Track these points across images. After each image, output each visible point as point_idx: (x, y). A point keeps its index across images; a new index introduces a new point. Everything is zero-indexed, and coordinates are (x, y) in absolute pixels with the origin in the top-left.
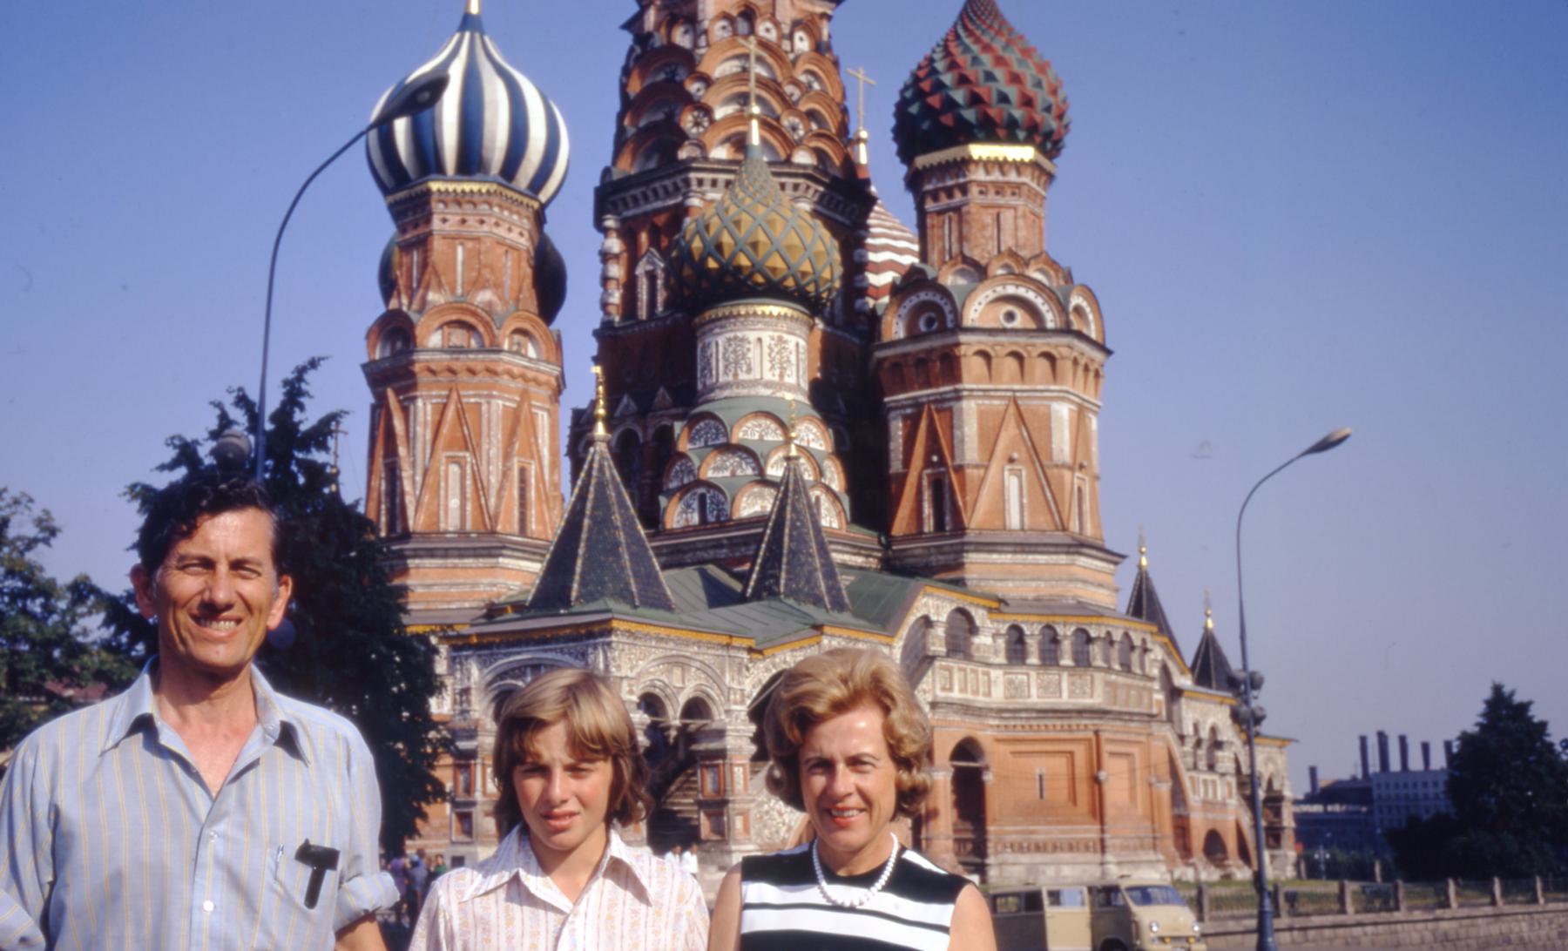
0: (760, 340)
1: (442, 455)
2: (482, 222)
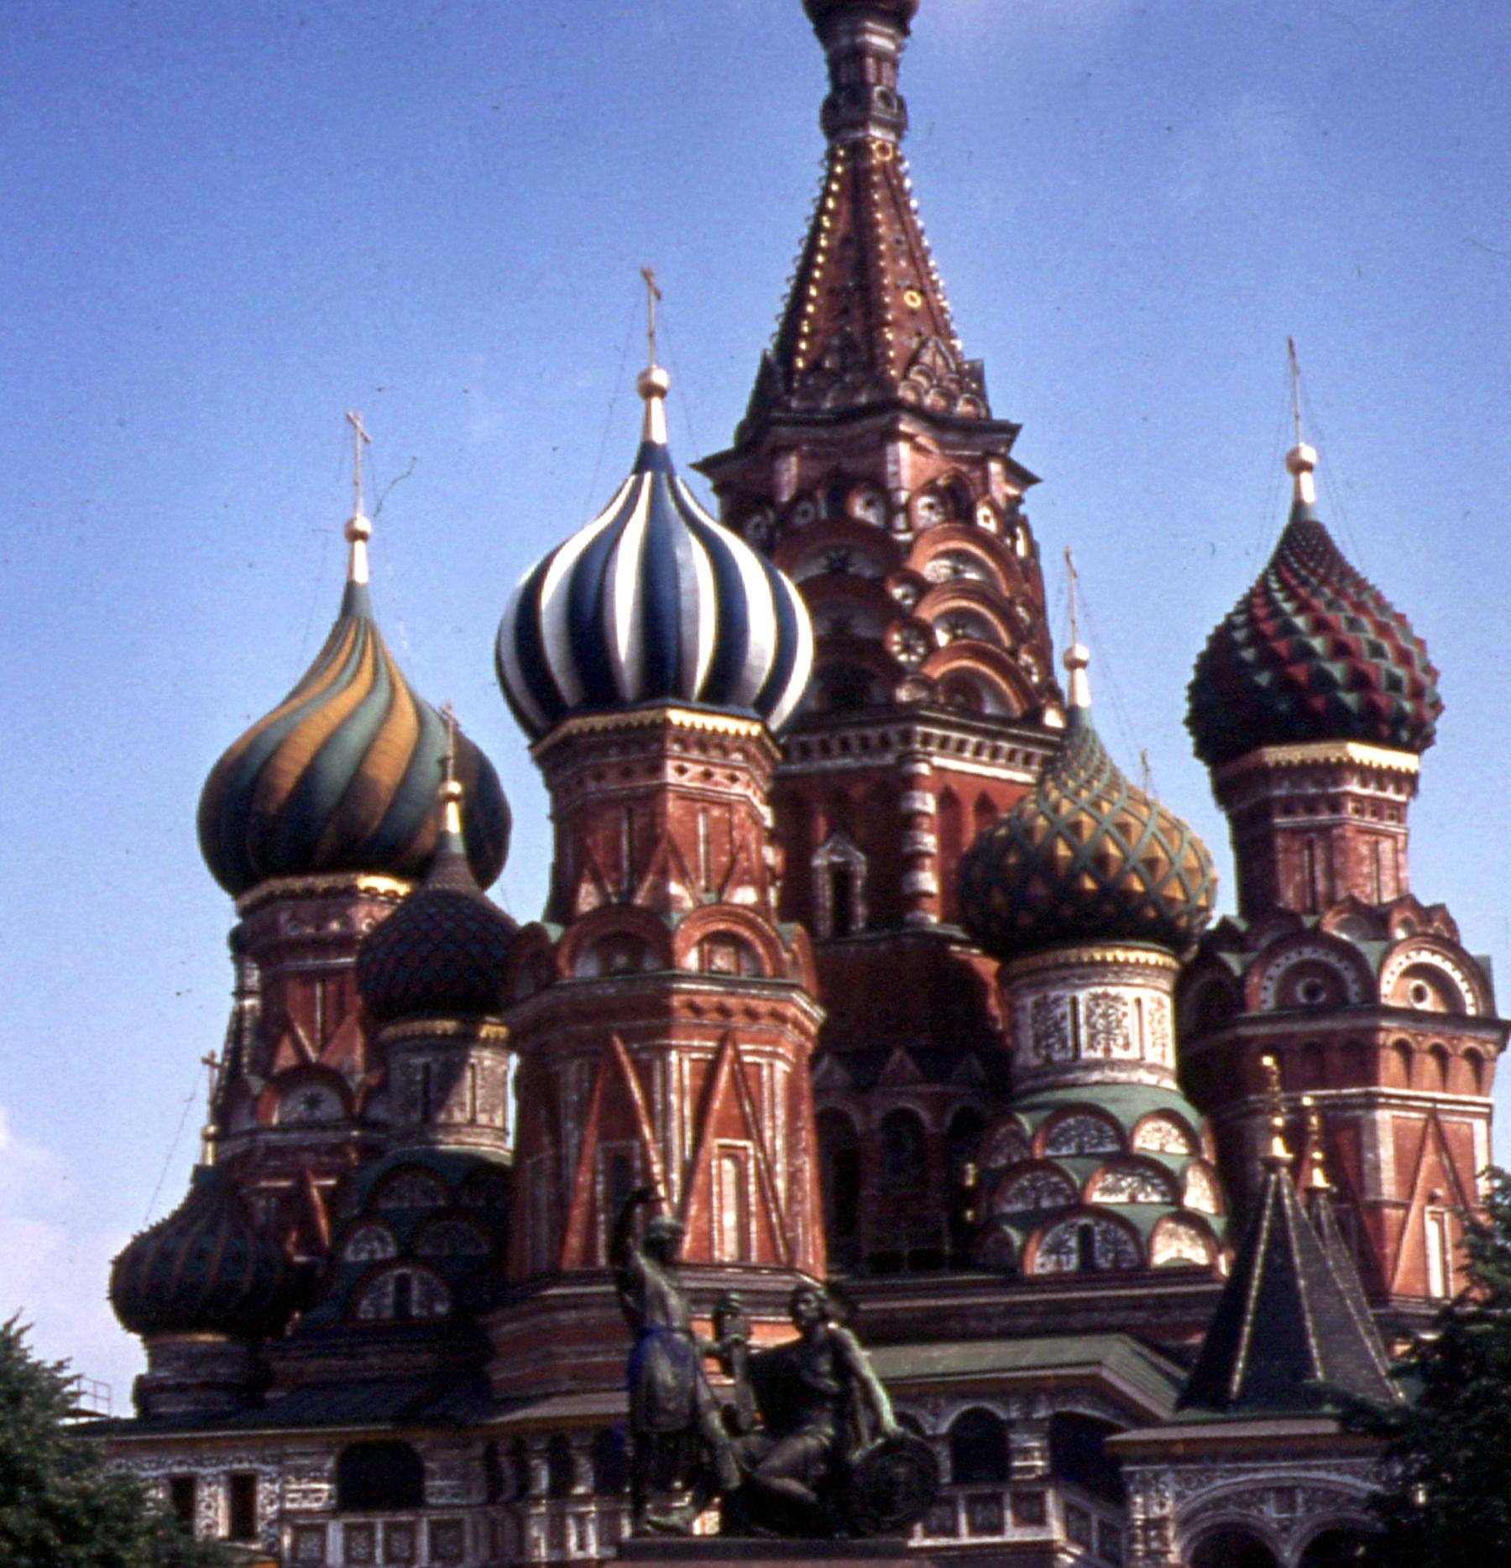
0: (1139, 1002)
1: (714, 1143)
2: (733, 779)
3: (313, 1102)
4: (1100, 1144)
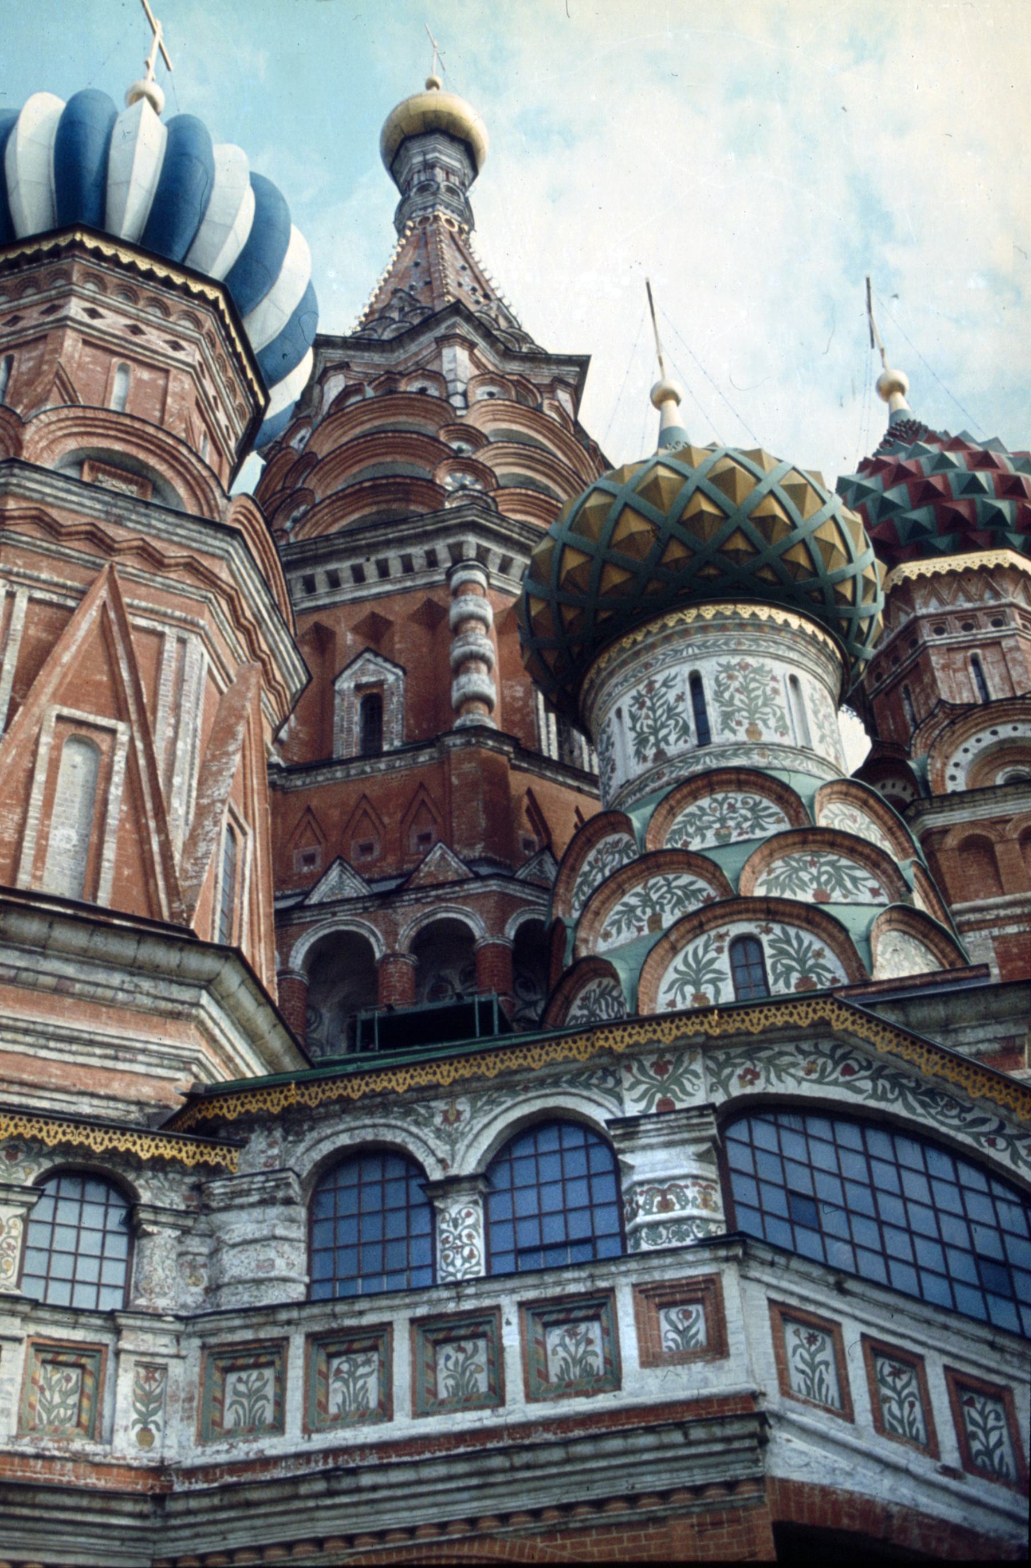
0: (794, 680)
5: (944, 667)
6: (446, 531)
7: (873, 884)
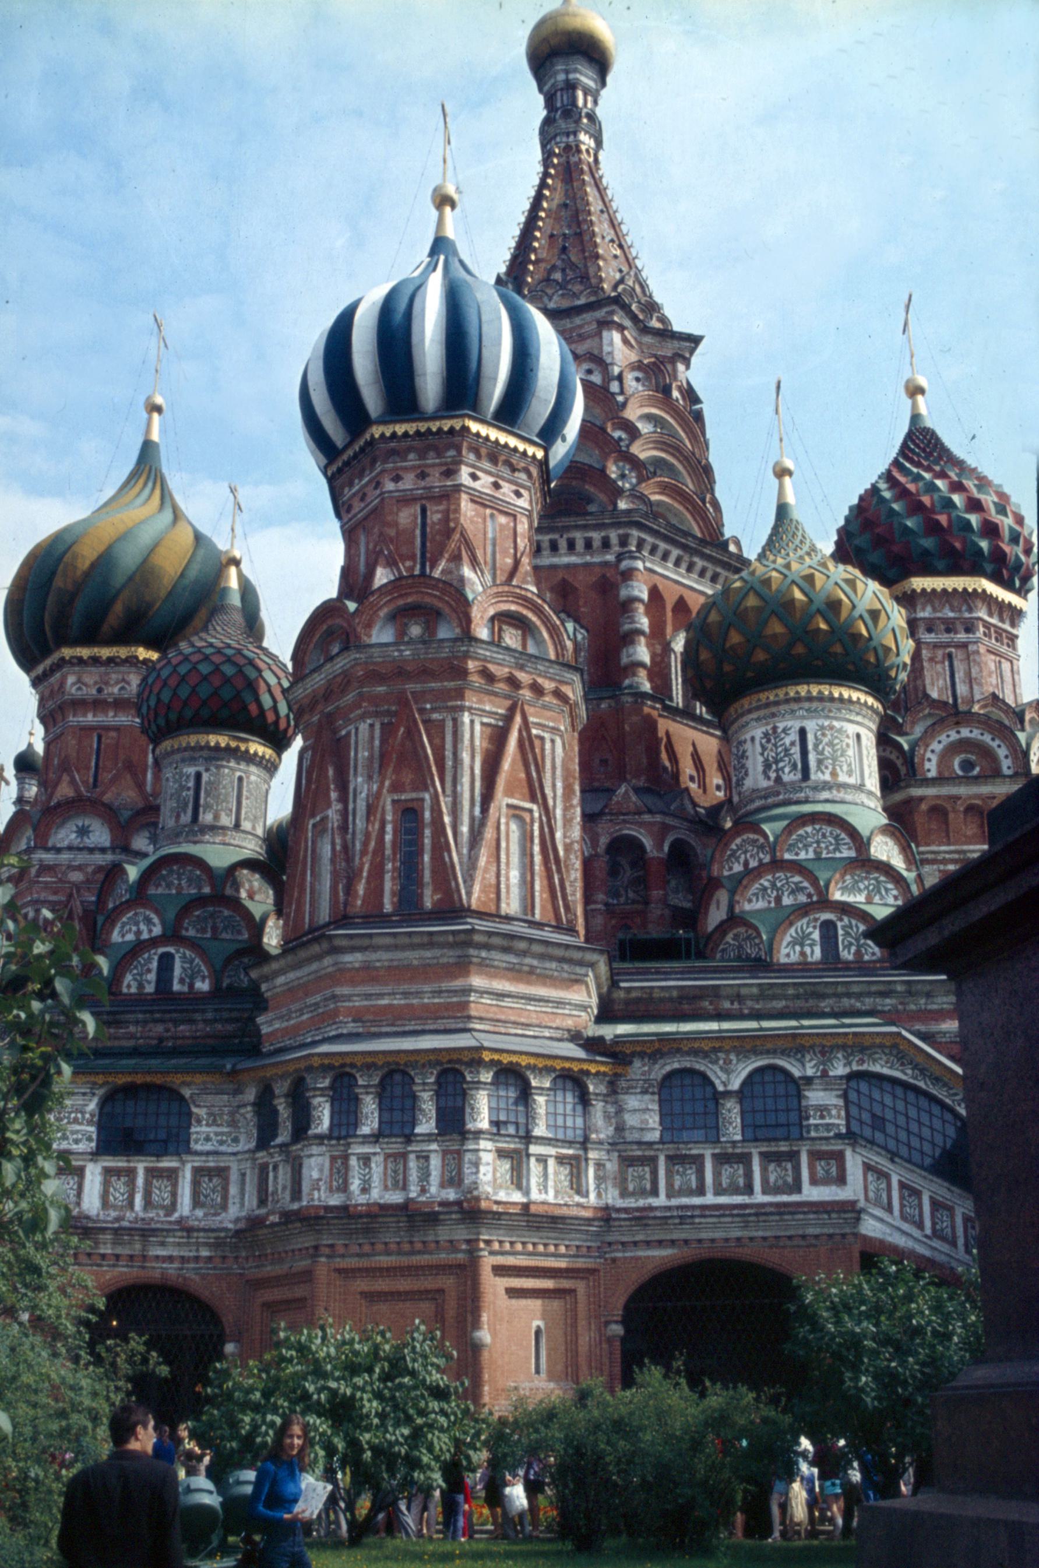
0: (858, 736)
1: (502, 800)
3: (83, 832)
4: (837, 849)
5: (931, 659)
6: (617, 525)
7: (895, 892)
